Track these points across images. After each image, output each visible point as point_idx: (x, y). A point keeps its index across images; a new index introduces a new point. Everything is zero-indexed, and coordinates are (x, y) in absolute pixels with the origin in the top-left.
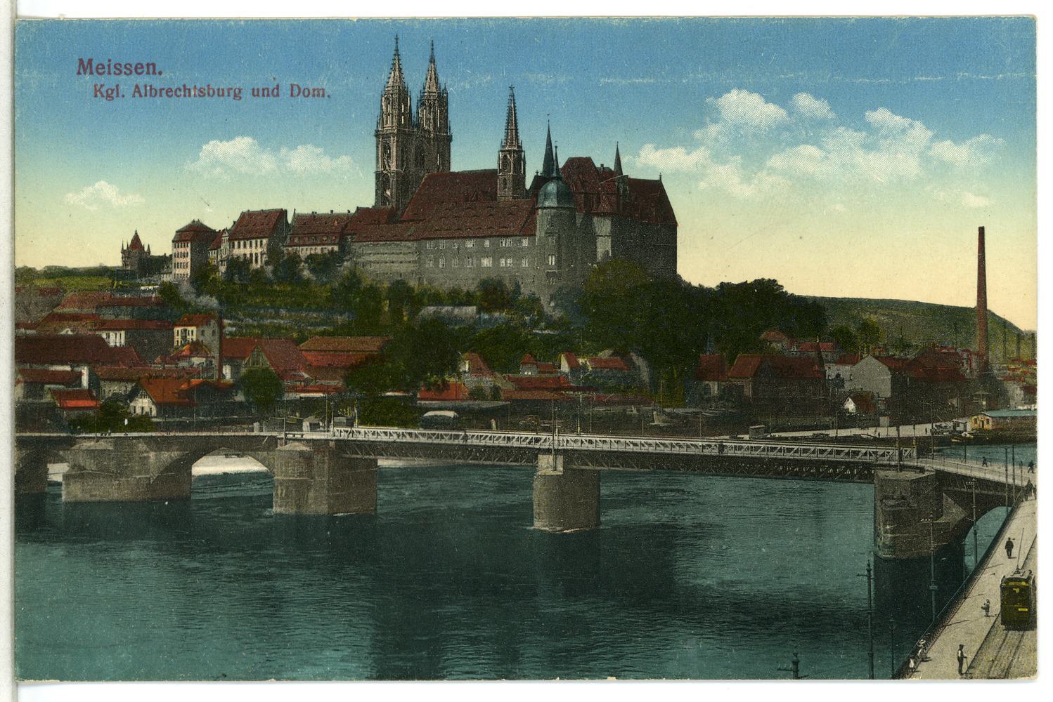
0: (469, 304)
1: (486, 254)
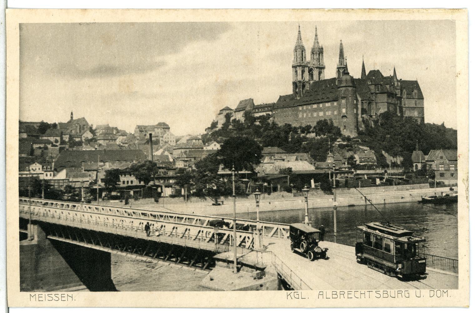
0: (313, 132)
1: (321, 110)
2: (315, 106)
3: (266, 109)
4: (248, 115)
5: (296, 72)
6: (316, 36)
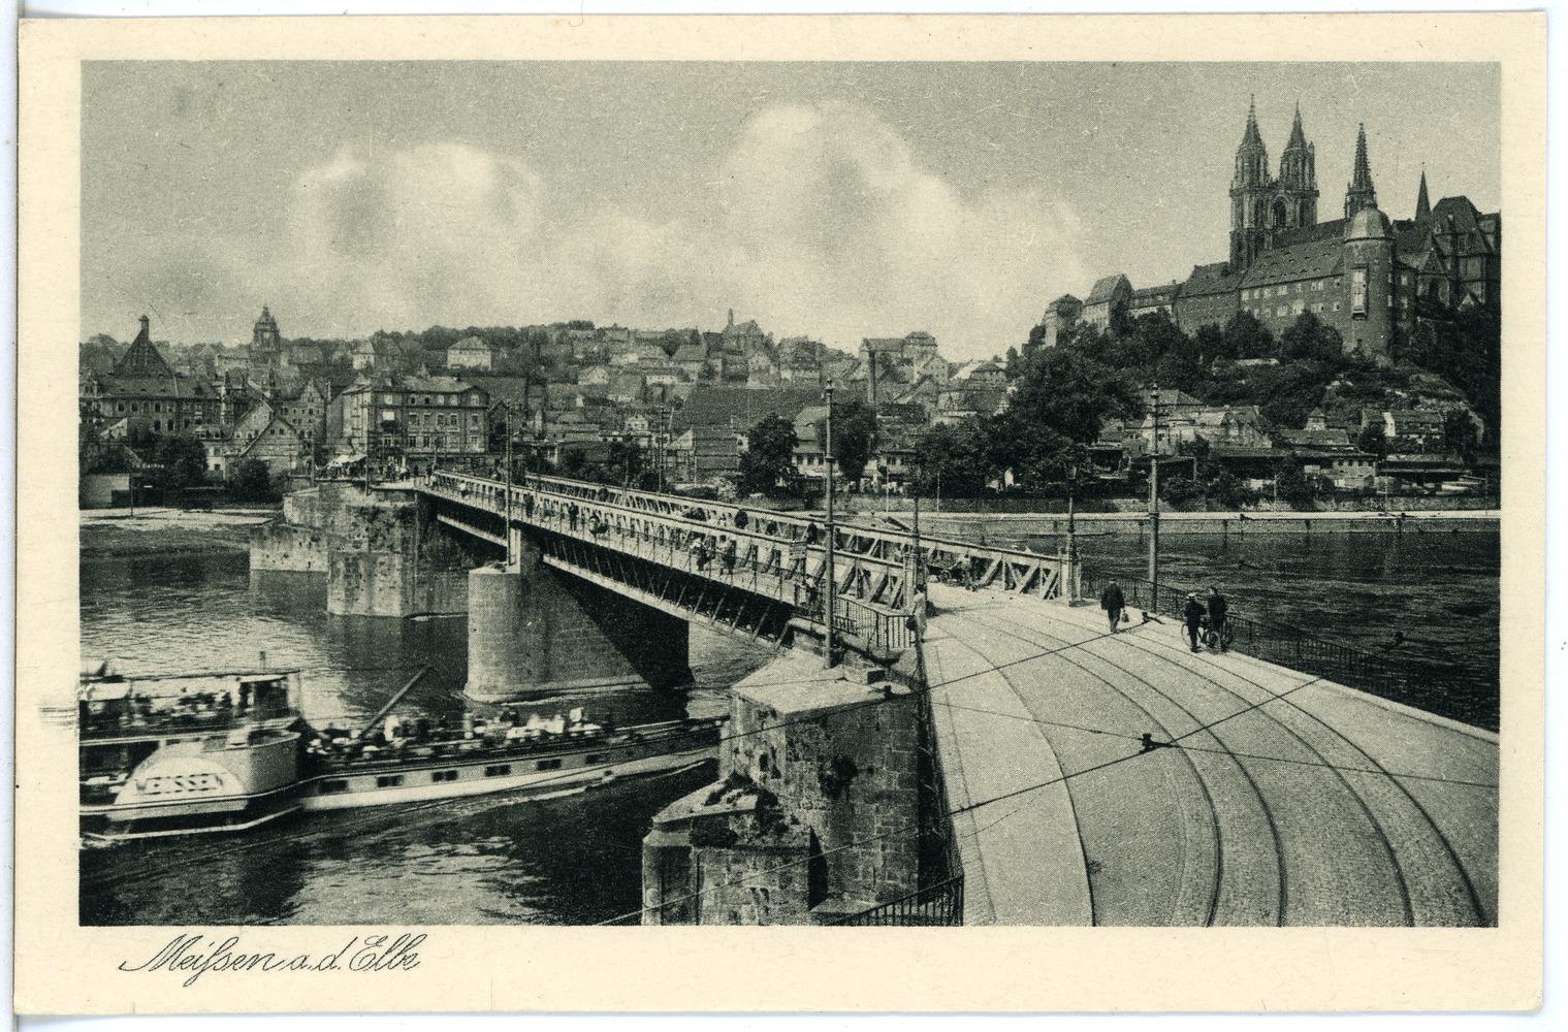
2: (1283, 291)
4: (1119, 313)
6: (1298, 114)
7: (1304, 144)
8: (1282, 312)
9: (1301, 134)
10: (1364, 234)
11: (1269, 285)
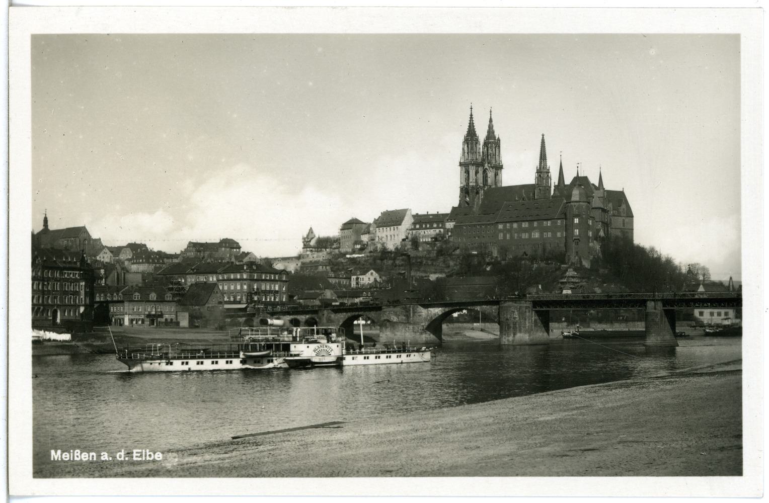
2: (525, 225)
3: (435, 226)
5: (467, 172)
6: (491, 121)
7: (495, 137)
8: (525, 236)
9: (493, 132)
10: (577, 199)
11: (516, 222)
